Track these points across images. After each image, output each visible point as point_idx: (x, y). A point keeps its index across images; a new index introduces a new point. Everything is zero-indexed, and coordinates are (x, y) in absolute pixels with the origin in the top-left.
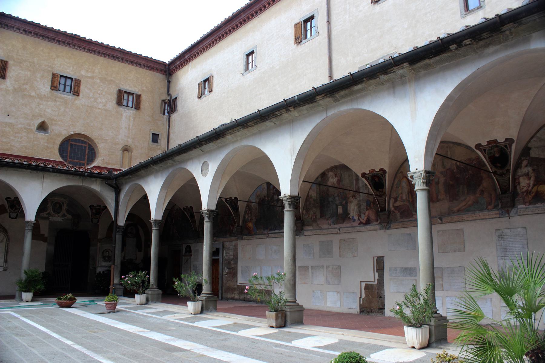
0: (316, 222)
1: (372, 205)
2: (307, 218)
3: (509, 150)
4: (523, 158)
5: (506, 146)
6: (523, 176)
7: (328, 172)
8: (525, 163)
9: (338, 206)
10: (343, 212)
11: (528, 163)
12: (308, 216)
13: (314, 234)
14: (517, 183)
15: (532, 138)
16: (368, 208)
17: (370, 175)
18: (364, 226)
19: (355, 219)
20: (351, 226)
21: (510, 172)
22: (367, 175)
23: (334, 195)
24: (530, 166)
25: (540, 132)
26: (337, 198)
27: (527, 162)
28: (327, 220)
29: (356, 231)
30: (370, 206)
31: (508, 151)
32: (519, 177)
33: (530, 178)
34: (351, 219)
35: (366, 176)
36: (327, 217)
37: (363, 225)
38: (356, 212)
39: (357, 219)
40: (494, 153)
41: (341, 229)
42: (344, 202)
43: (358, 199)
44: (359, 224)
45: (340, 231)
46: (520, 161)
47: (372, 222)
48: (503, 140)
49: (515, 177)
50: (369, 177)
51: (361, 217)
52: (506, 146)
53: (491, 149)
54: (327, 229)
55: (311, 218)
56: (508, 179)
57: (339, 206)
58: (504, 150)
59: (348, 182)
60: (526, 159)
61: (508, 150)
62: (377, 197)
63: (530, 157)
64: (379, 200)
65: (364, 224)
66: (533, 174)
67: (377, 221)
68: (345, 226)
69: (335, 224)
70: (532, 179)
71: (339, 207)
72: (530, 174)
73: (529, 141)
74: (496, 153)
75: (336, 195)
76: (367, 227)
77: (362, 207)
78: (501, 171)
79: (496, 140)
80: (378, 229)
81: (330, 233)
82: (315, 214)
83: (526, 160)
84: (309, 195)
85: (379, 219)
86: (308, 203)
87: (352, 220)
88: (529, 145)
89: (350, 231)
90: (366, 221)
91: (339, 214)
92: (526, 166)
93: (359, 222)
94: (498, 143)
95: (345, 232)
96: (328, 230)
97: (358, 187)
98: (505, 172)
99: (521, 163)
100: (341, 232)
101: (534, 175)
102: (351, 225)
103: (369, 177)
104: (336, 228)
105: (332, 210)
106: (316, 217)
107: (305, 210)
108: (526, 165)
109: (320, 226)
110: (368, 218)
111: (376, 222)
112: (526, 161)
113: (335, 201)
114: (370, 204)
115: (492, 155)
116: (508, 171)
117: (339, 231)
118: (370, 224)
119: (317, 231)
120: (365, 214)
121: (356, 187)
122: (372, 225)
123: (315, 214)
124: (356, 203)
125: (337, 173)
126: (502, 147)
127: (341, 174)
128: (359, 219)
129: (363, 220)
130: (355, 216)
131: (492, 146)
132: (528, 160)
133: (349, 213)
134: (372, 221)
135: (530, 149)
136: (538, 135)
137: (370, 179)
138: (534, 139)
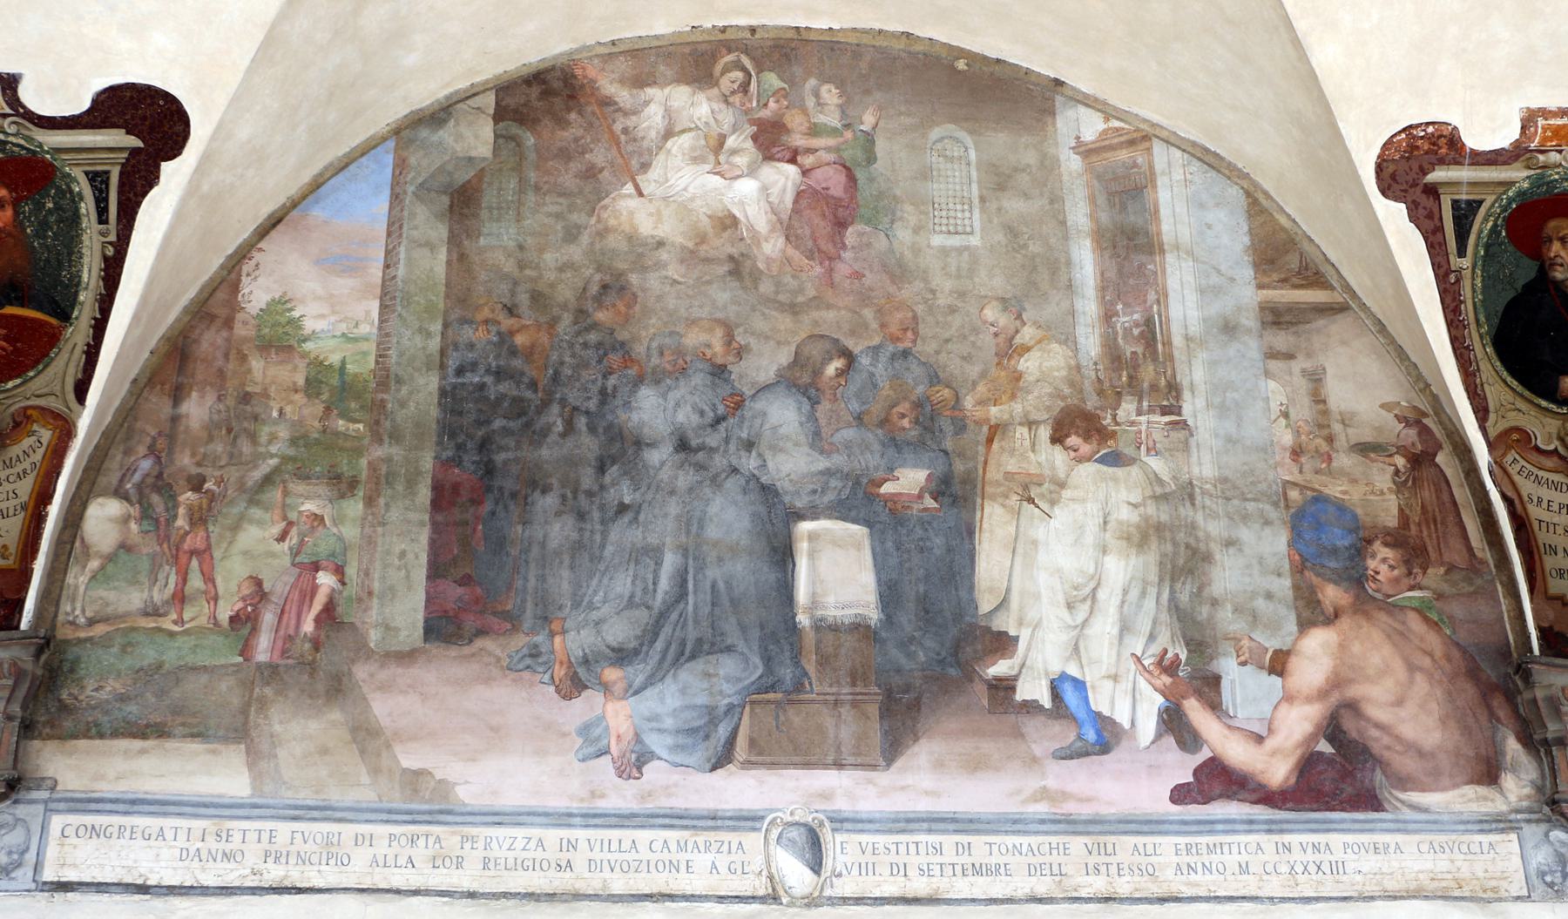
0: (337, 689)
1: (1382, 562)
2: (153, 612)
7: (640, 81)
9: (800, 516)
10: (889, 594)
12: (180, 598)
13: (274, 874)
16: (1332, 594)
17: (1512, 183)
18: (1271, 828)
19: (1122, 717)
20: (1041, 808)
22: (1464, 173)
23: (719, 372)
26: (783, 414)
28: (573, 686)
29: (1124, 887)
30: (1357, 579)
34: (1031, 707)
35: (1438, 175)
36: (575, 641)
37: (1261, 812)
38: (1125, 628)
39: (1148, 726)
41: (841, 849)
42: (910, 479)
43: (1155, 463)
44: (1180, 795)
45: (816, 866)
47: (1404, 782)
50: (1474, 205)
51: (1215, 706)
54: (562, 819)
55: (244, 622)
57: (813, 513)
59: (975, 241)
62: (1516, 462)
64: (1535, 512)
65: (1269, 798)
67: (1489, 773)
68: (923, 805)
69: (722, 760)
71: (805, 527)
75: (765, 363)
76: (1336, 839)
77: (1227, 576)
80: (1518, 887)
81: (618, 886)
82: (325, 580)
84: (234, 307)
85: (1512, 746)
86: (197, 409)
87: (1065, 735)
89: (1022, 885)
90: (1308, 764)
91: (803, 619)
93: (1181, 768)
95: (919, 886)
96: (580, 834)
97: (1150, 335)
100: (846, 887)
102: (1044, 794)
103: (1474, 205)
104: (747, 820)
105: (670, 561)
106: (329, 614)
107: (119, 493)
109: (409, 759)
110: (1333, 729)
111: (1470, 791)
113: (749, 445)
114: (1360, 550)
117: (795, 874)
118: (1369, 801)
119: (348, 830)
120: (1278, 665)
121: (1108, 316)
122: (1402, 828)
123: (325, 580)
124: (1126, 515)
125: (795, 121)
127: (869, 140)
128: (1174, 723)
129: (1259, 739)
130: (1115, 678)
133: (1006, 623)
134: (1406, 764)
137: (1481, 226)
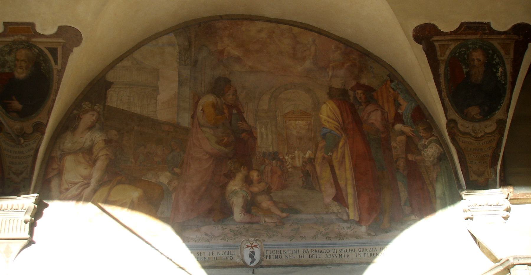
3: (59, 66)
4: (84, 106)
5: (53, 51)
6: (74, 153)
8: (88, 118)
11: (98, 120)
14: (55, 172)
15: (121, 59)
21: (43, 133)
24: (102, 129)
25: (147, 47)
27: (94, 118)
31: (55, 68)
32: (64, 154)
33: (93, 163)
40: (15, 66)
46: (75, 112)
48: (51, 30)
49: (53, 154)
52: (56, 49)
53: (7, 49)
56: (32, 153)
58: (46, 60)
60: (94, 110)
61: (56, 63)
63: (105, 106)
66: (104, 152)
70: (100, 164)
72: (95, 151)
73: (112, 66)
74: (21, 67)
78: (17, 126)
79: (32, 25)
83: (95, 113)
88: (110, 77)
92: (90, 128)
94: (34, 37)
98: (30, 130)
99: (78, 118)
101: (107, 155)
108: (90, 124)
112: (93, 115)
115: (7, 70)
116: (40, 128)
126: (41, 51)
131: (14, 42)
132: (98, 113)
135: (109, 85)
136: (136, 55)
138: (126, 63)
